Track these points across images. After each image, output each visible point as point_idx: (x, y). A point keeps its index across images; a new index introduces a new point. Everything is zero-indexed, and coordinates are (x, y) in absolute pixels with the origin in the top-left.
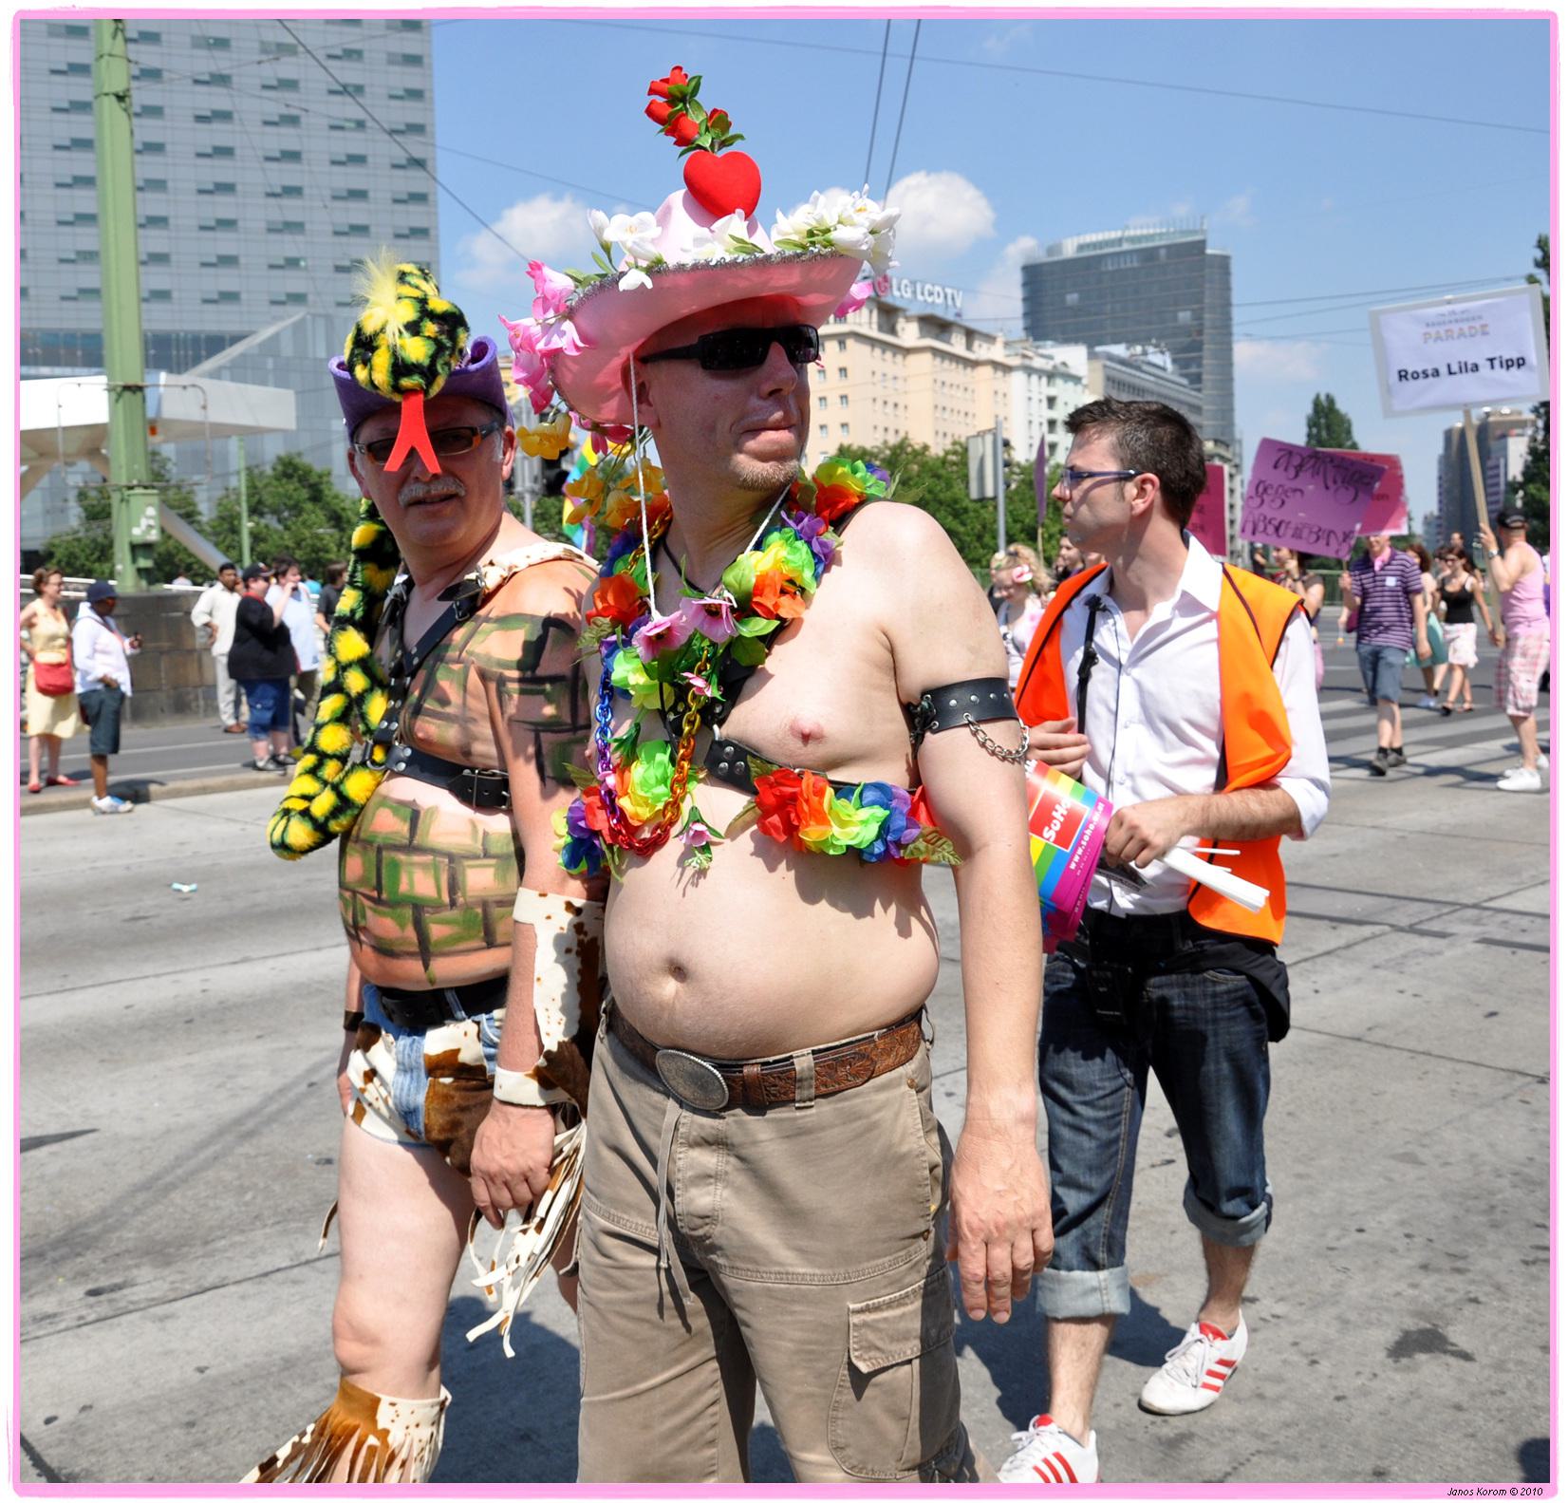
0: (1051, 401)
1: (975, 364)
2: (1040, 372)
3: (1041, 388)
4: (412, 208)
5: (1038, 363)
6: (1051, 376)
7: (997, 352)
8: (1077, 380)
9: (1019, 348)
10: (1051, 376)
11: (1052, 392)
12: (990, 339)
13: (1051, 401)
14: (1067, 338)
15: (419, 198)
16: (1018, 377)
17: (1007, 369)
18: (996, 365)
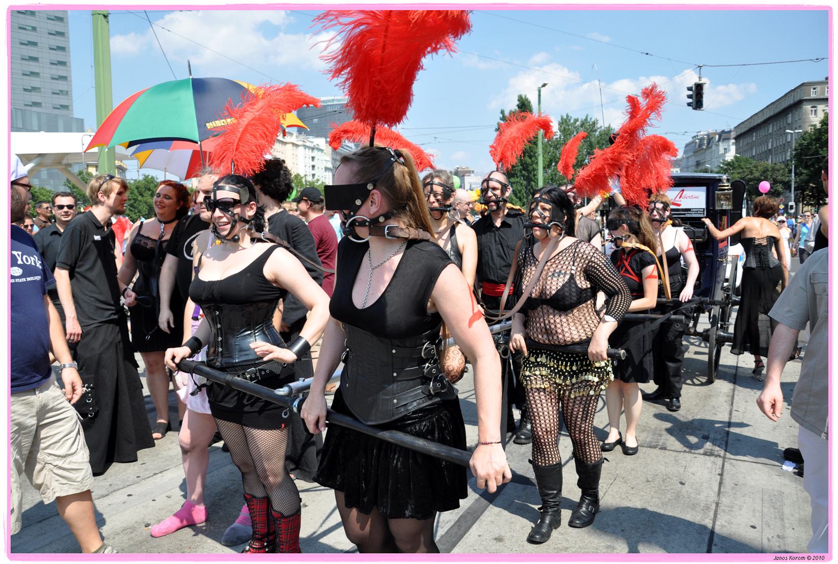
0: (313, 158)
1: (285, 143)
2: (309, 147)
3: (310, 153)
4: (59, 67)
5: (308, 144)
6: (313, 149)
7: (293, 139)
8: (322, 151)
9: (302, 137)
10: (313, 149)
11: (313, 155)
12: (291, 134)
13: (313, 158)
14: (317, 136)
15: (63, 63)
16: (301, 148)
17: (297, 146)
18: (293, 144)
